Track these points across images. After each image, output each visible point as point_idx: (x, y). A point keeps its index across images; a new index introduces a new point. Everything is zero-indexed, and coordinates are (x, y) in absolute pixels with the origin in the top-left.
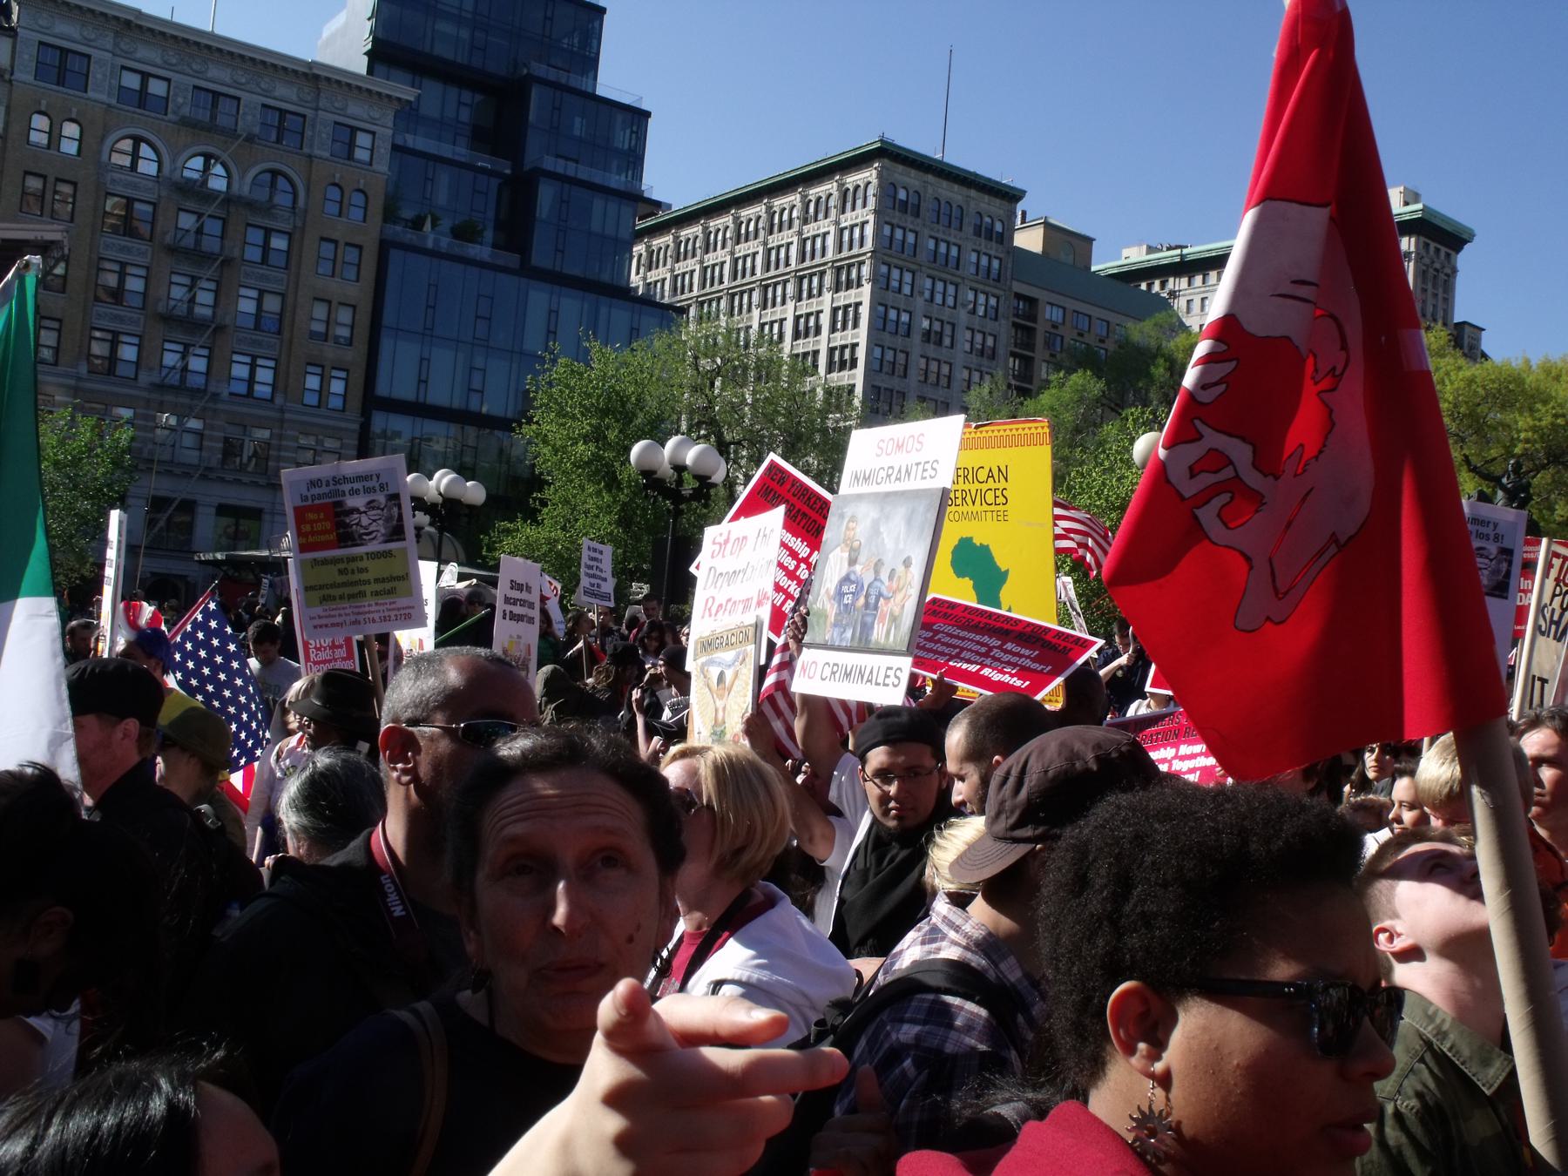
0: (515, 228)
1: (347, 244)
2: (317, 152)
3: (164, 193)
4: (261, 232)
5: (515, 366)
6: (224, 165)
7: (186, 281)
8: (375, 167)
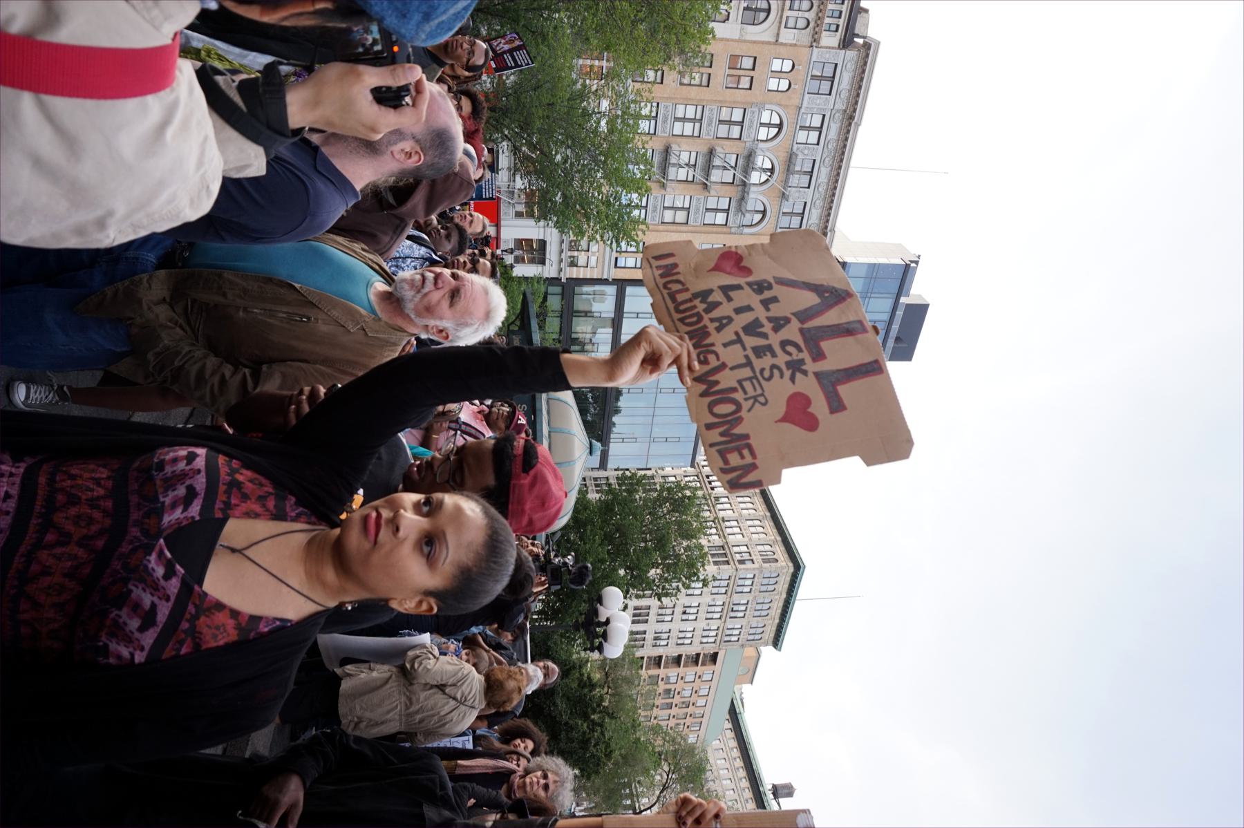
3: (748, 145)
7: (692, 162)
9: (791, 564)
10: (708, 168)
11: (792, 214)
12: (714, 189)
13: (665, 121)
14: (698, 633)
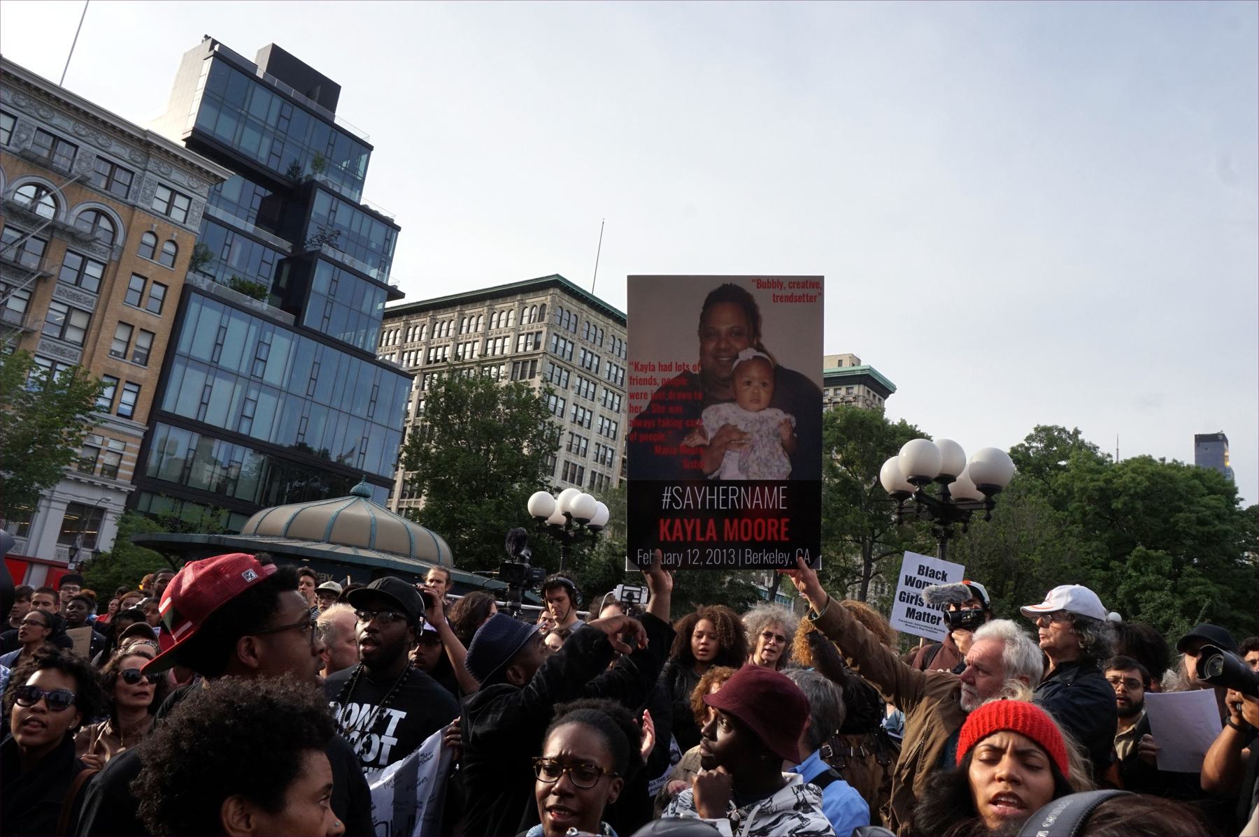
0: (291, 291)
1: (155, 282)
2: (140, 204)
4: (80, 259)
5: (281, 402)
6: (54, 198)
8: (188, 225)
9: (551, 291)
11: (110, 179)
12: (50, 267)
14: (606, 413)
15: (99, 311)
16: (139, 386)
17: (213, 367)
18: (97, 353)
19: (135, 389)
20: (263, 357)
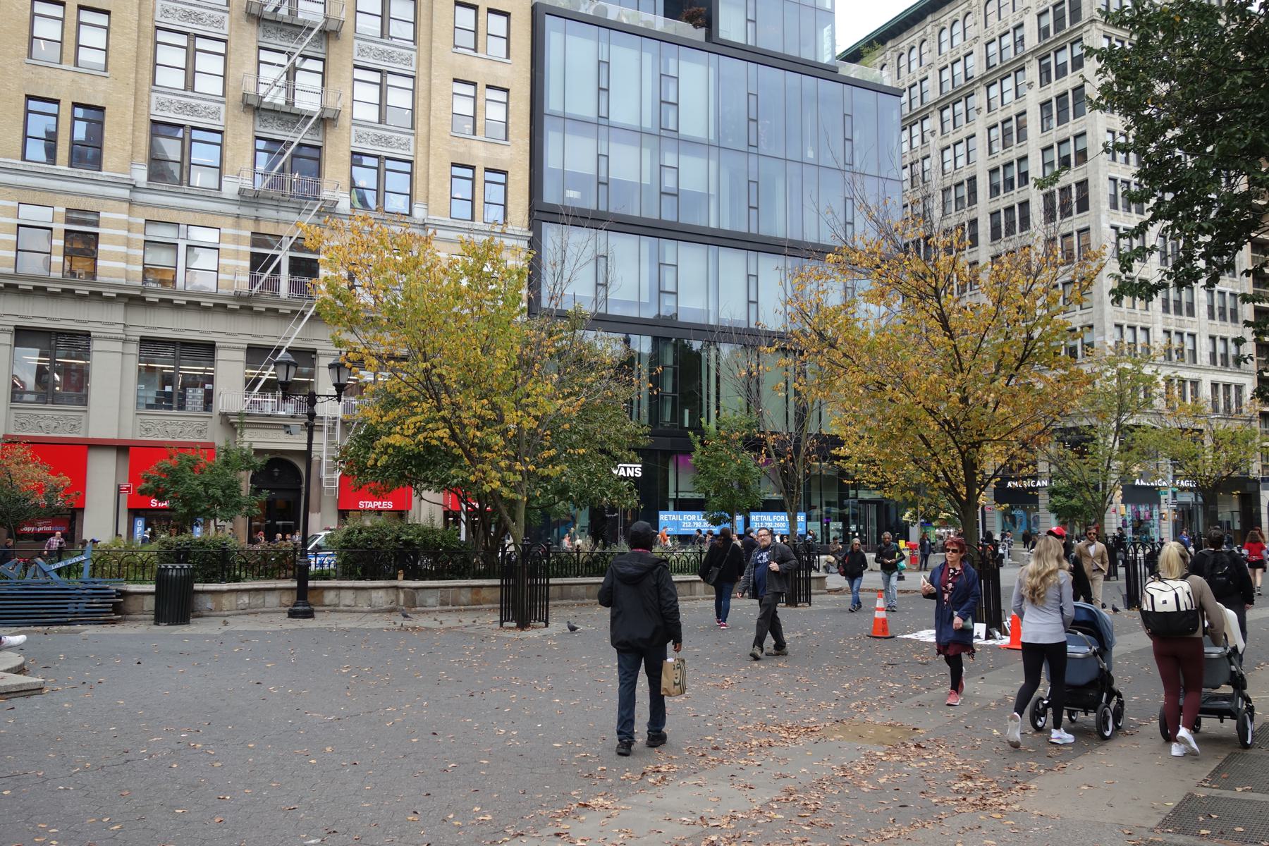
1: (491, 11)
5: (713, 164)
10: (294, 28)
13: (193, 110)
15: (423, 70)
16: (505, 173)
17: (601, 124)
18: (434, 134)
19: (501, 178)
20: (672, 99)
